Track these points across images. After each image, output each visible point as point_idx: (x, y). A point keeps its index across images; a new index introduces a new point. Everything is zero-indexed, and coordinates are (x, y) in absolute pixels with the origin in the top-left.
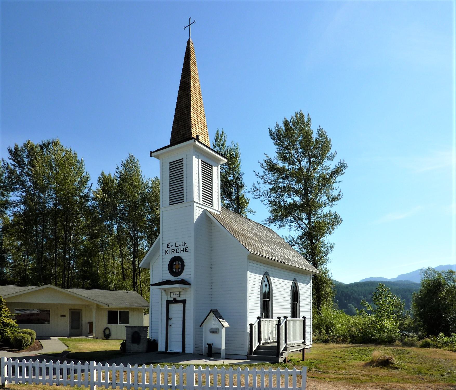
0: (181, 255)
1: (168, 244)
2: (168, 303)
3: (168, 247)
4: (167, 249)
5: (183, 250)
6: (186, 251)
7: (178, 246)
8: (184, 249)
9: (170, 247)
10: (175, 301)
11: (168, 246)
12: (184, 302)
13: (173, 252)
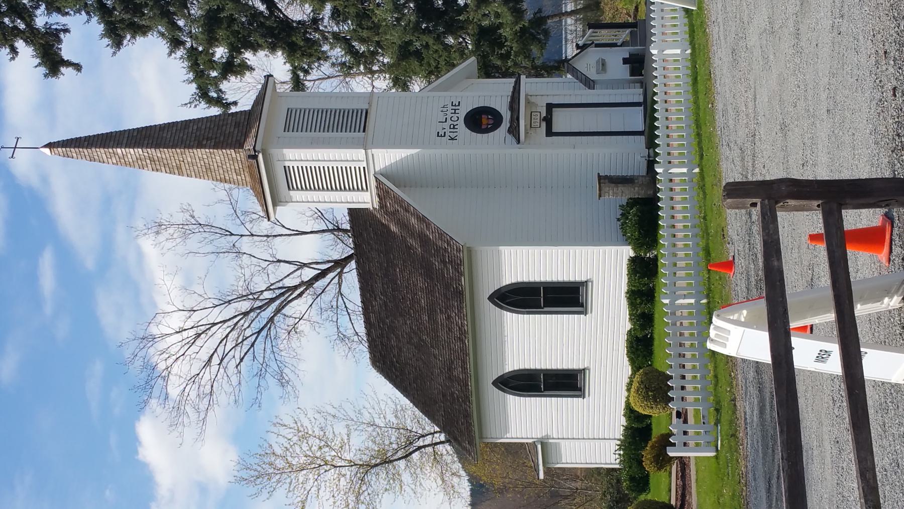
0: (462, 113)
1: (438, 136)
2: (550, 133)
3: (444, 136)
4: (447, 137)
5: (455, 110)
6: (457, 104)
7: (446, 118)
8: (454, 108)
9: (445, 133)
10: (548, 120)
11: (441, 136)
12: (550, 107)
13: (456, 127)
